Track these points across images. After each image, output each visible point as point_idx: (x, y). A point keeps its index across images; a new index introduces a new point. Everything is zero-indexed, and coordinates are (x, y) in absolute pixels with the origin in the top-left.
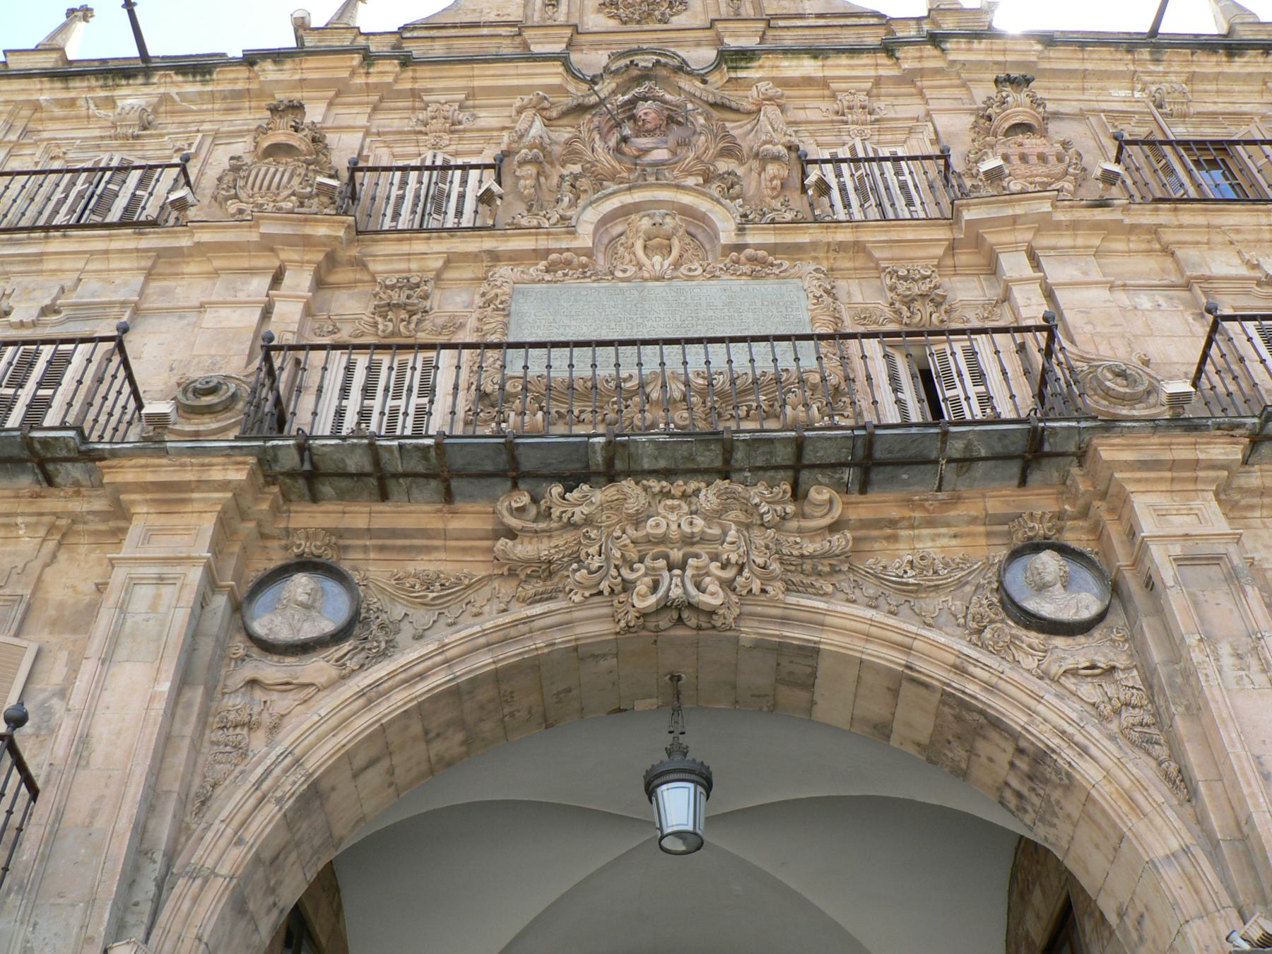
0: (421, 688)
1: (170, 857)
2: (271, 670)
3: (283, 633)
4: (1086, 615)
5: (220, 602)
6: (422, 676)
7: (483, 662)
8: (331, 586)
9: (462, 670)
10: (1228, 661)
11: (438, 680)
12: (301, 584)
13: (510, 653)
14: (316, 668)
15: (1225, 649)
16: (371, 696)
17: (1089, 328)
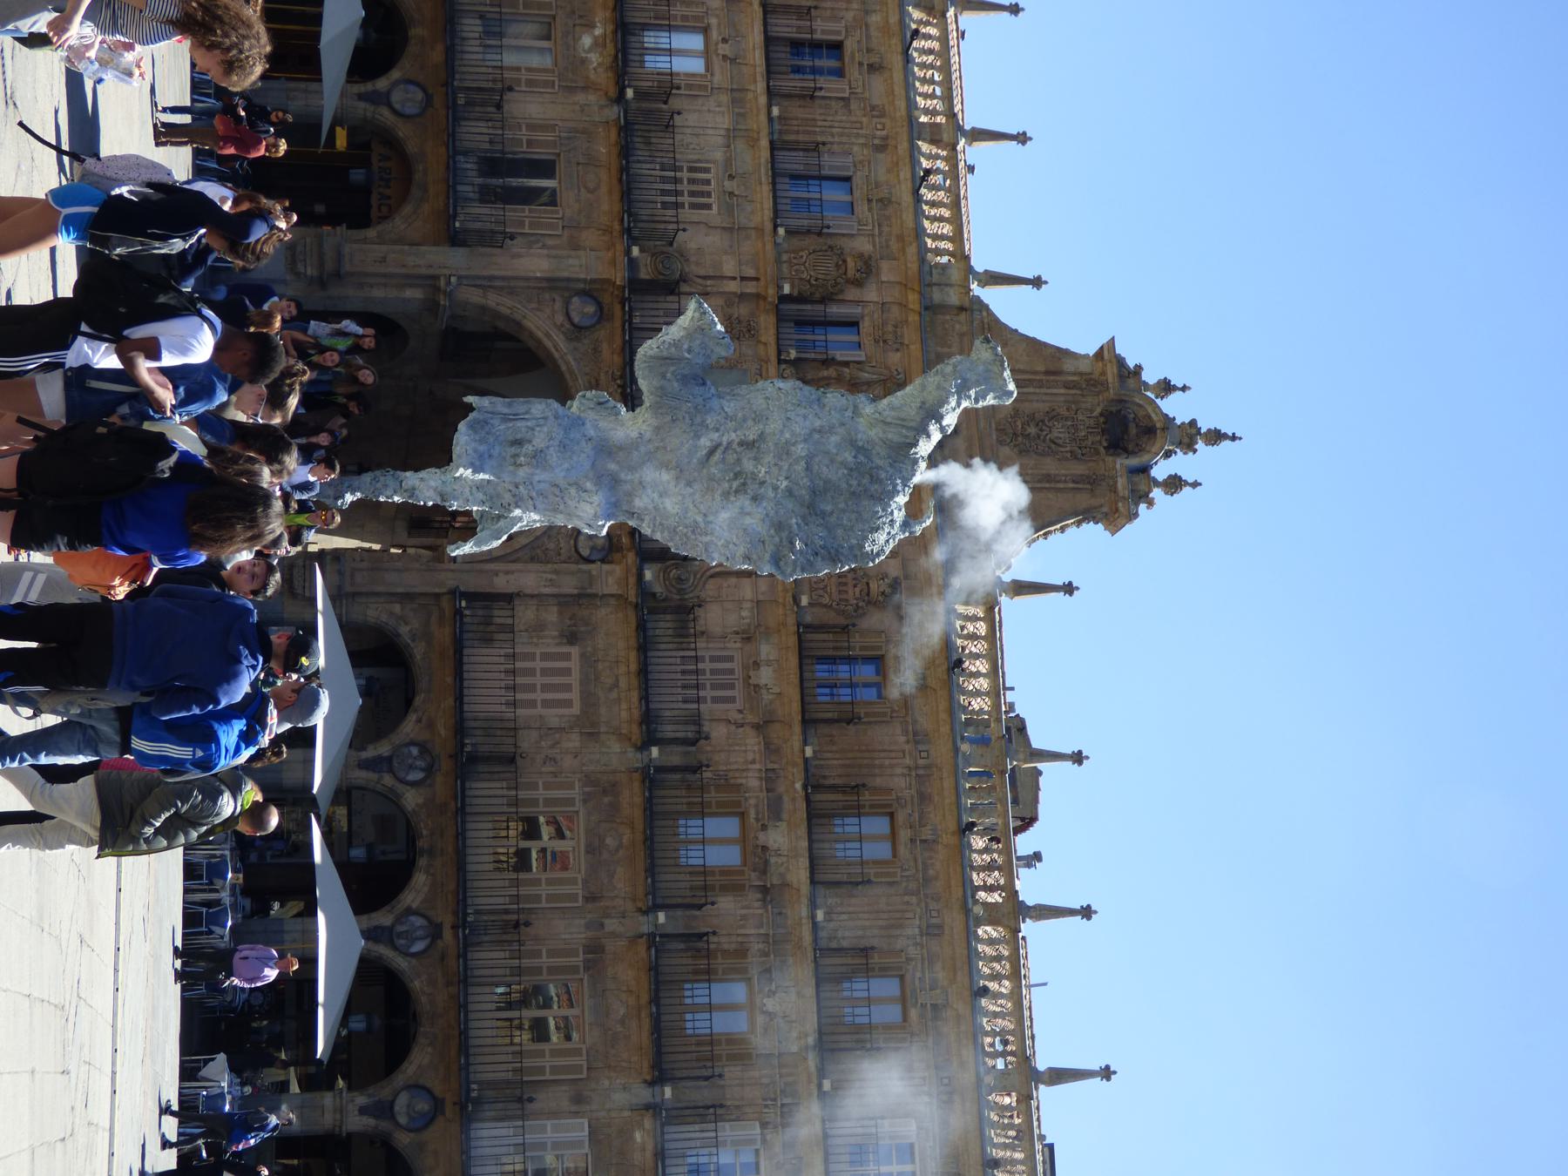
0: (553, 350)
1: (490, 287)
2: (558, 305)
3: (572, 307)
4: (581, 550)
5: (582, 286)
6: (557, 350)
7: (564, 368)
8: (596, 318)
9: (560, 362)
10: (549, 576)
11: (556, 355)
12: (591, 309)
13: (567, 376)
14: (560, 318)
15: (554, 577)
16: (548, 335)
17: (725, 585)
